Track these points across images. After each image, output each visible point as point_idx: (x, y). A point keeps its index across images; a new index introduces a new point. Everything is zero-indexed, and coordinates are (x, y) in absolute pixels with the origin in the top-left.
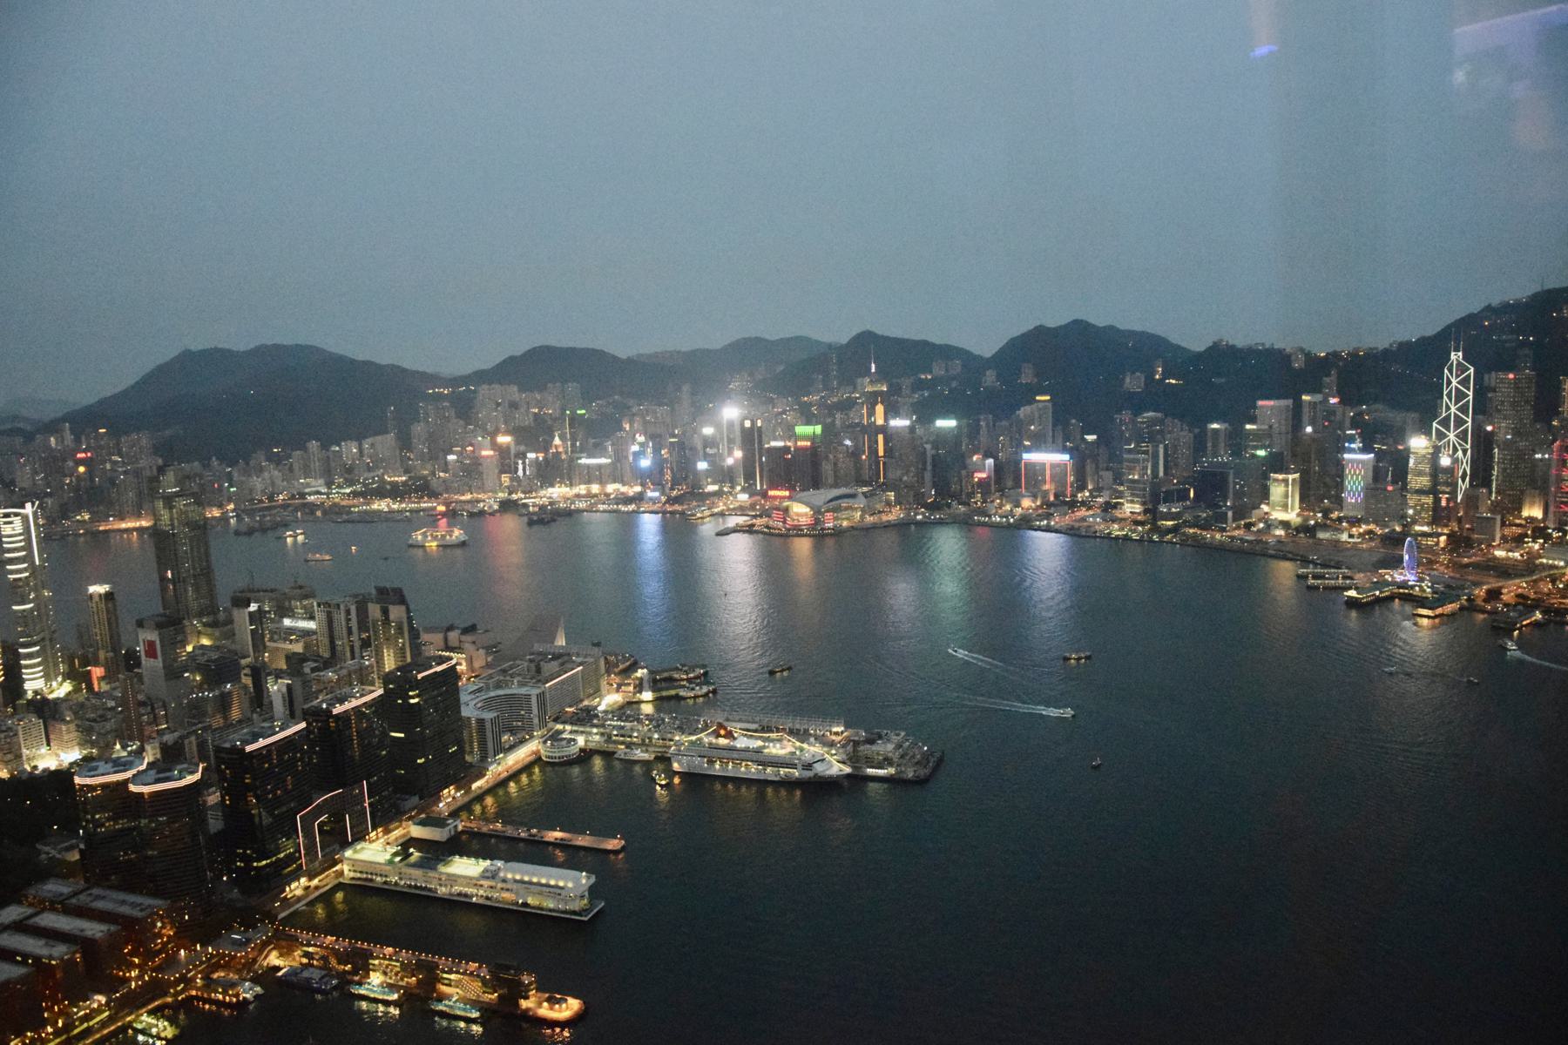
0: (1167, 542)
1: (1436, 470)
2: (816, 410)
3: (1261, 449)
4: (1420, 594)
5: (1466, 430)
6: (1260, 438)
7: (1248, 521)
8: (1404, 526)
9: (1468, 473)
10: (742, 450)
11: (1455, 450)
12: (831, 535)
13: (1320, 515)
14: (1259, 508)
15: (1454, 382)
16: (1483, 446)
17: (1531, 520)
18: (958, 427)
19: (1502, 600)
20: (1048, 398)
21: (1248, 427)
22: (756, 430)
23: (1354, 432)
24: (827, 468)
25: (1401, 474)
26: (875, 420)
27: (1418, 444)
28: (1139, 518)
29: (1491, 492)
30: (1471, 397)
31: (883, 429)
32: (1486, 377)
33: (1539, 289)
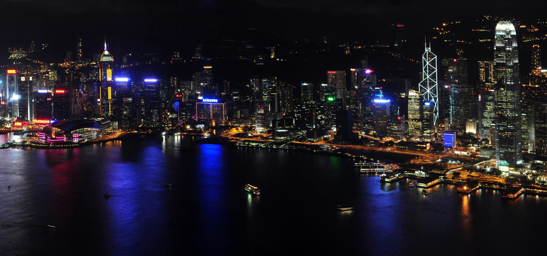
0: (281, 149)
1: (421, 110)
2: (68, 71)
3: (330, 97)
4: (419, 175)
6: (331, 91)
7: (325, 136)
8: (408, 139)
9: (438, 110)
10: (19, 94)
11: (431, 98)
12: (77, 147)
13: (364, 133)
14: (331, 129)
15: (428, 63)
16: (444, 95)
17: (470, 134)
18: (157, 83)
19: (460, 177)
20: (211, 67)
21: (323, 85)
22: (28, 83)
23: (379, 88)
24: (76, 107)
25: (404, 111)
26: (106, 77)
27: (412, 93)
28: (265, 135)
29: (450, 119)
30: (436, 71)
31: (113, 84)
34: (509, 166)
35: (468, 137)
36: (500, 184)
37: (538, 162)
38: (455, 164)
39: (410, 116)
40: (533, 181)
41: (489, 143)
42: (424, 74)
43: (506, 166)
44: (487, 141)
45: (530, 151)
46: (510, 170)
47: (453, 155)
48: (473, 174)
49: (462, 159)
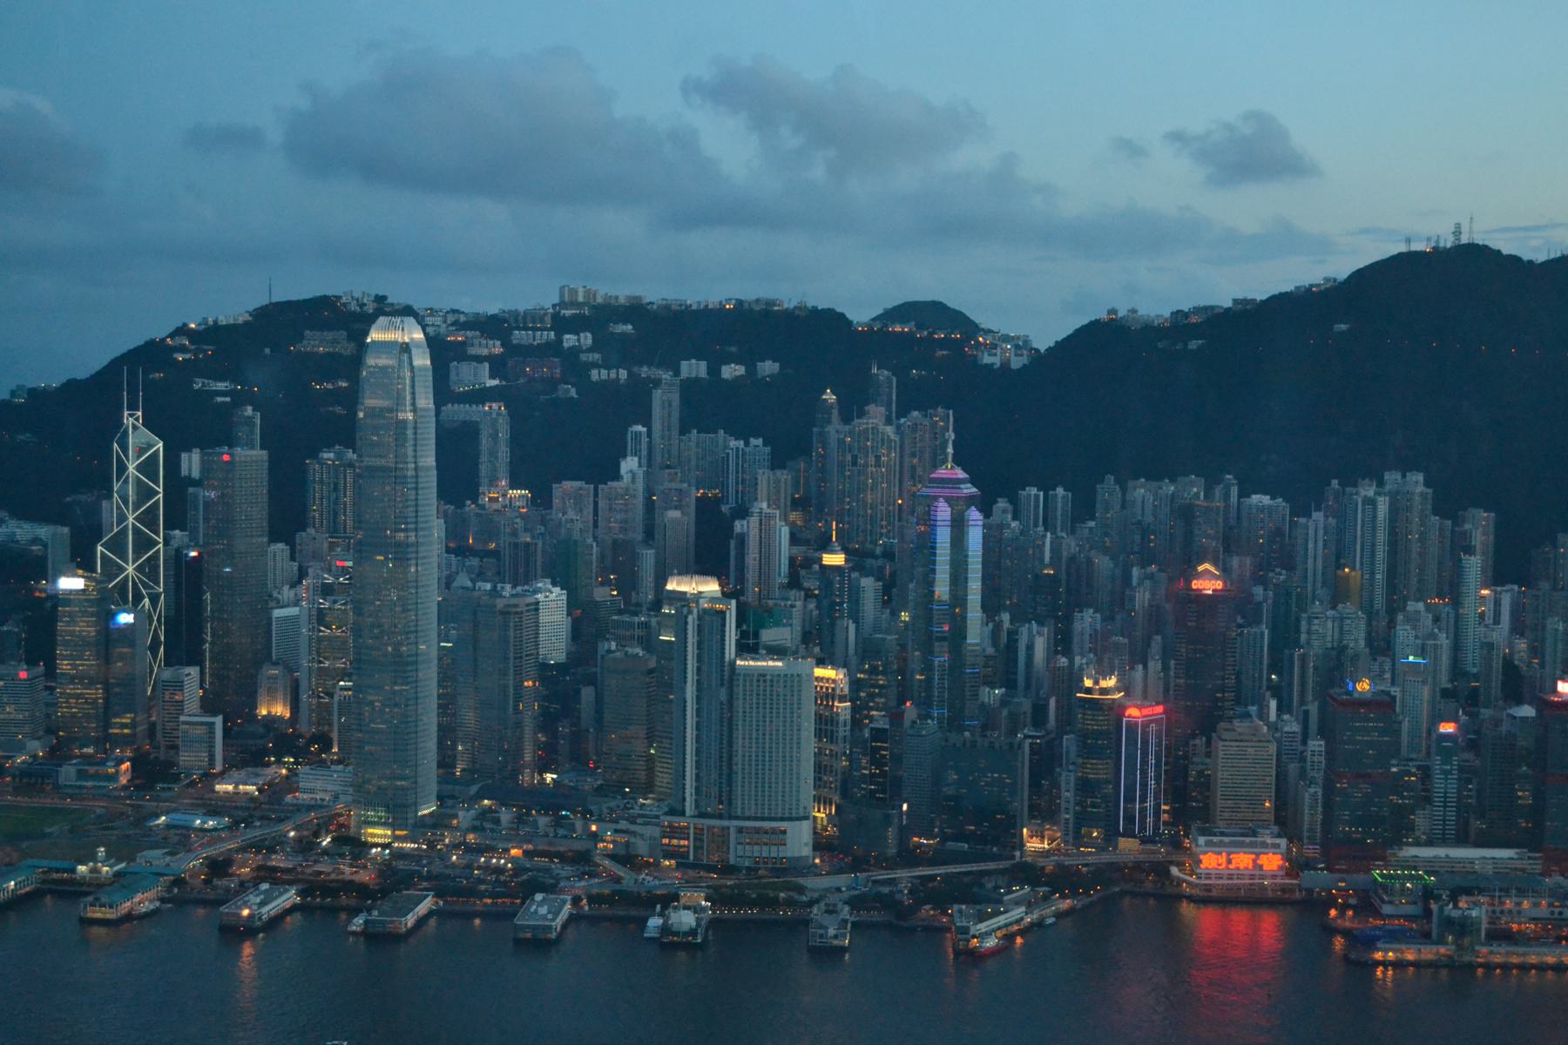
5: (156, 556)
11: (138, 598)
15: (131, 468)
17: (271, 720)
30: (161, 495)
32: (184, 456)
33: (265, 302)
34: (393, 827)
35: (261, 730)
36: (362, 890)
37: (486, 802)
38: (215, 829)
39: (64, 666)
40: (469, 867)
41: (332, 748)
42: (119, 508)
43: (385, 825)
44: (326, 745)
45: (463, 770)
46: (396, 838)
47: (211, 799)
48: (277, 860)
49: (239, 813)
